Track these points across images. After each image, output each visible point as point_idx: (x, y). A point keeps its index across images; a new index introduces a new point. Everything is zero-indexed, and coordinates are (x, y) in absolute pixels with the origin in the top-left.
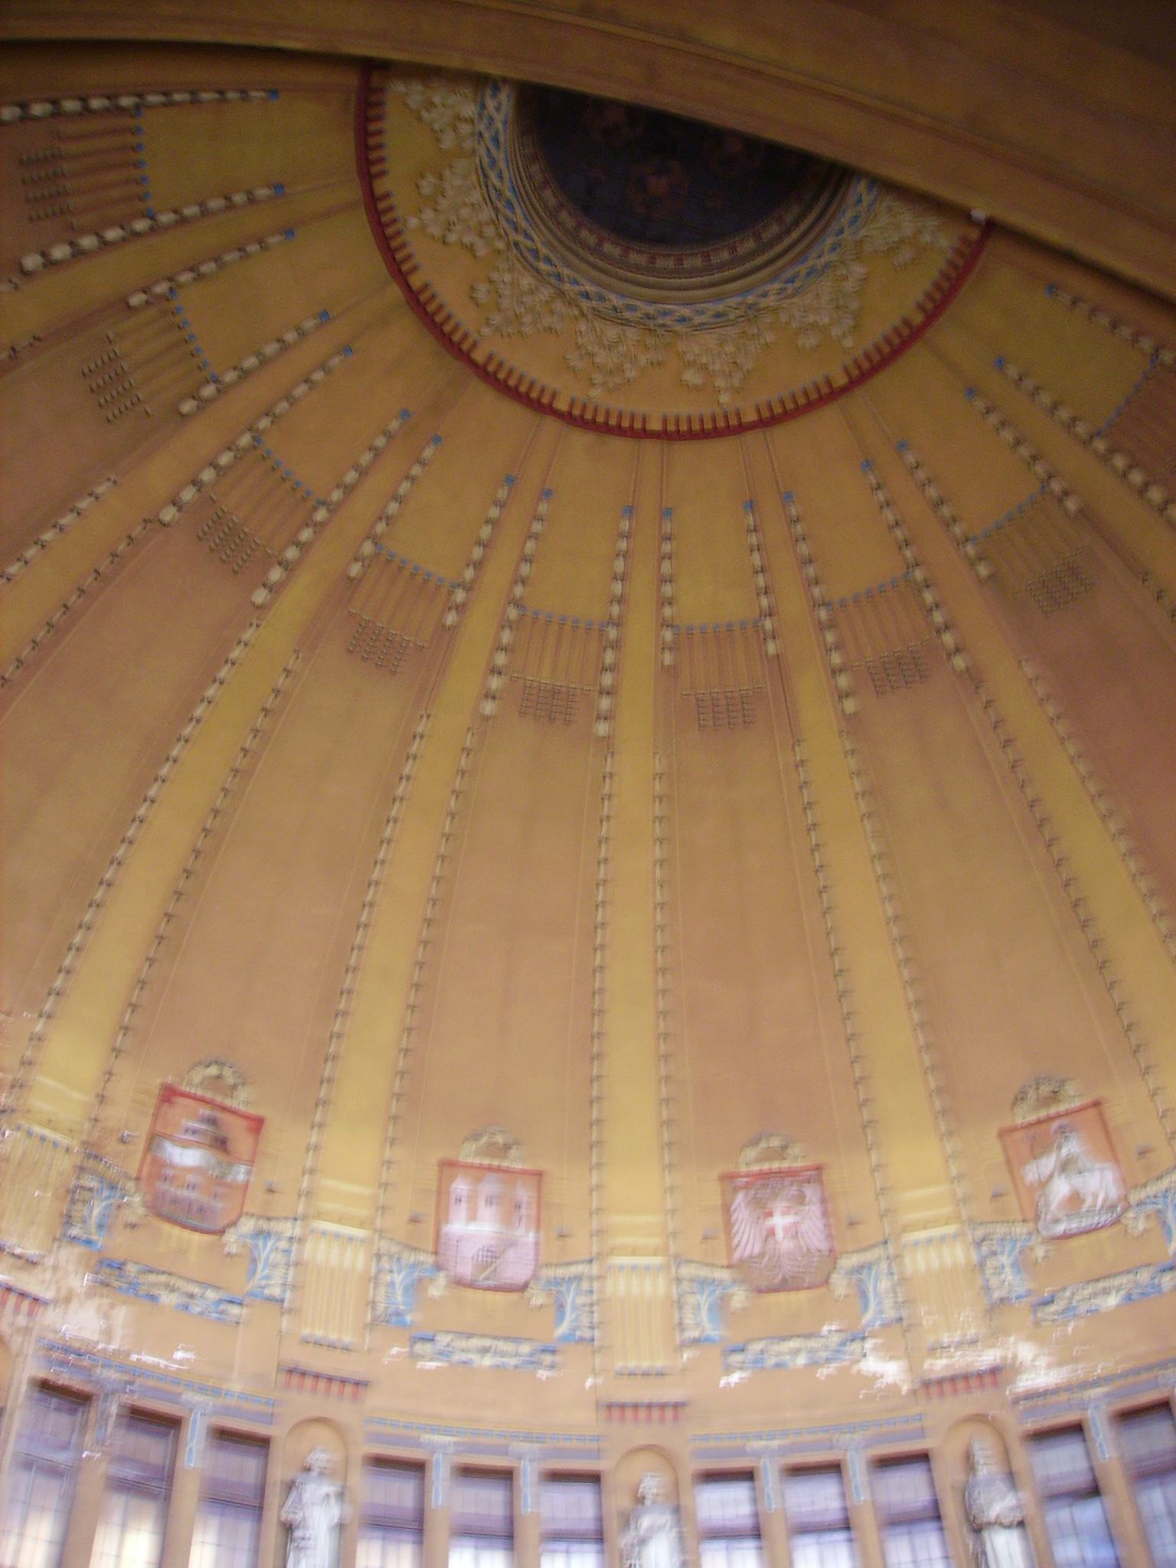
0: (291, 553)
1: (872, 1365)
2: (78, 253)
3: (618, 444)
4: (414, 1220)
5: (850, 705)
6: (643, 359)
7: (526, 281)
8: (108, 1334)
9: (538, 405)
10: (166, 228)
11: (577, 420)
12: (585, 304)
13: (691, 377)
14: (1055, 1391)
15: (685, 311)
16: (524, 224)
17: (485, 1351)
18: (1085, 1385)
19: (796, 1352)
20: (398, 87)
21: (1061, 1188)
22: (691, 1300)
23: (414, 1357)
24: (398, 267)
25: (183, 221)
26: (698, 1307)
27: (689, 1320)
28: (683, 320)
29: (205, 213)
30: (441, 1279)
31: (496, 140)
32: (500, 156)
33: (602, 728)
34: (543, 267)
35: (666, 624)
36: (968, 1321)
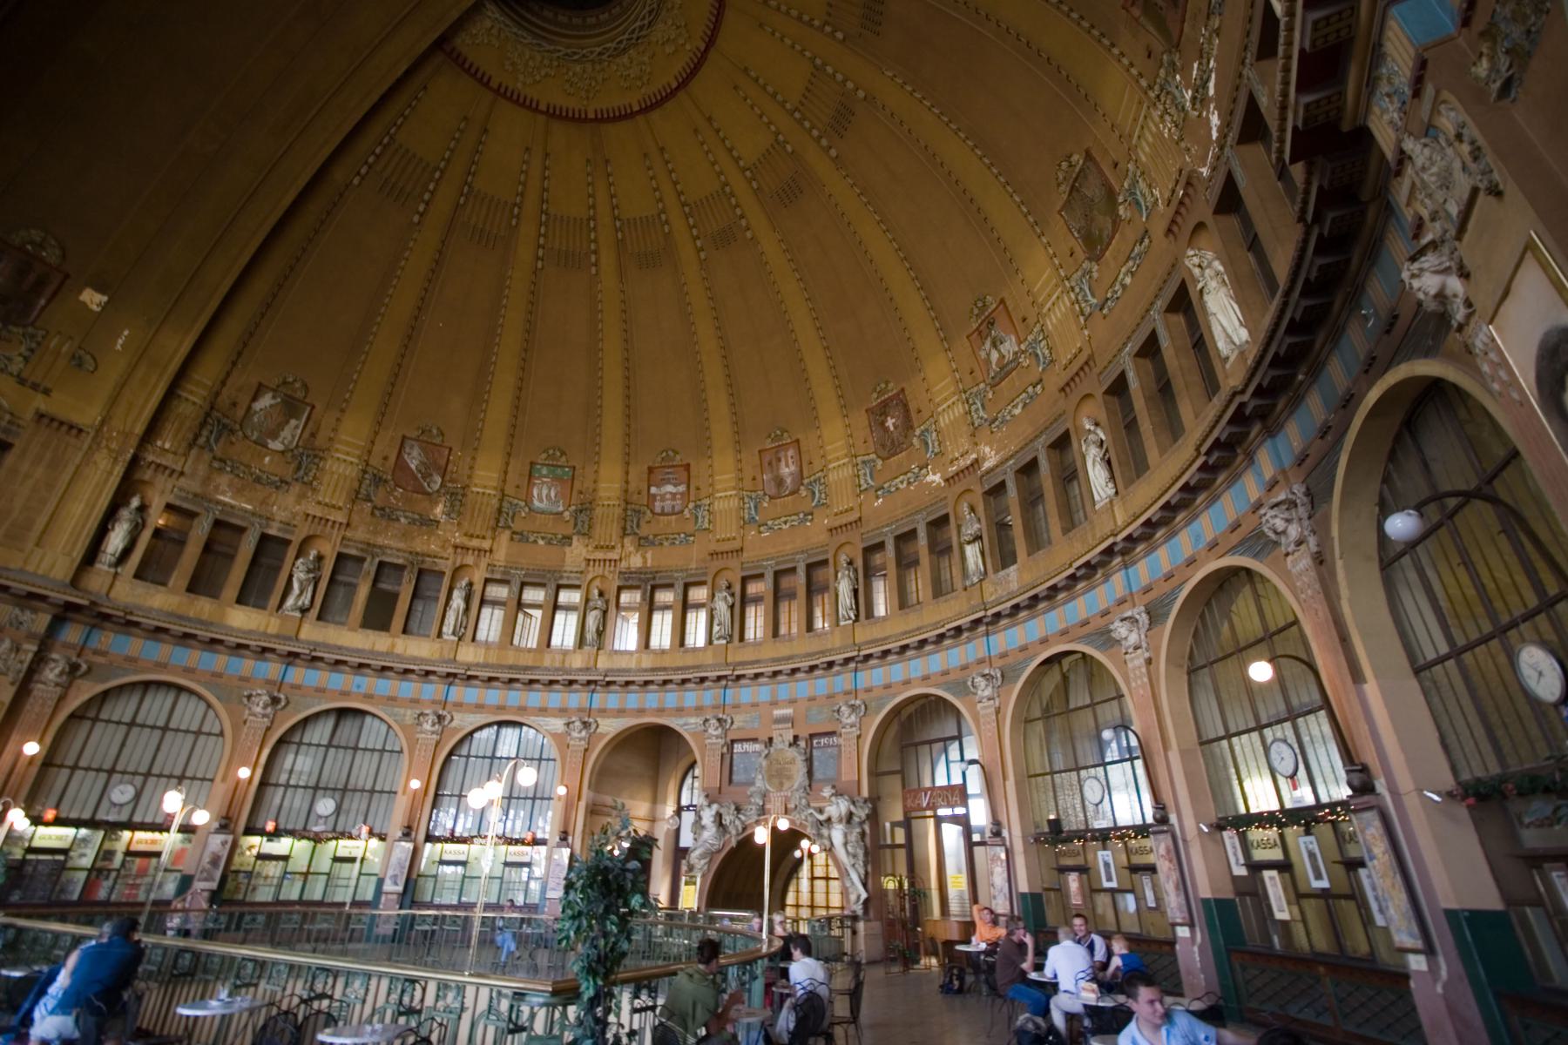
0: (593, 247)
1: (930, 478)
2: (427, 204)
3: (669, 105)
4: (754, 479)
5: (833, 153)
6: (646, 59)
7: (578, 68)
8: (645, 562)
9: (626, 116)
10: (446, 167)
11: (647, 109)
12: (604, 57)
13: (669, 49)
14: (997, 466)
15: (638, 24)
16: (552, 48)
17: (785, 523)
18: (1007, 460)
19: (902, 482)
20: (458, 42)
21: (995, 356)
22: (861, 473)
23: (760, 532)
24: (532, 107)
25: (448, 161)
26: (865, 474)
27: (862, 482)
28: (641, 28)
29: (452, 151)
30: (767, 498)
31: (507, 26)
32: (515, 30)
33: (749, 234)
34: (576, 57)
35: (744, 170)
36: (965, 443)
